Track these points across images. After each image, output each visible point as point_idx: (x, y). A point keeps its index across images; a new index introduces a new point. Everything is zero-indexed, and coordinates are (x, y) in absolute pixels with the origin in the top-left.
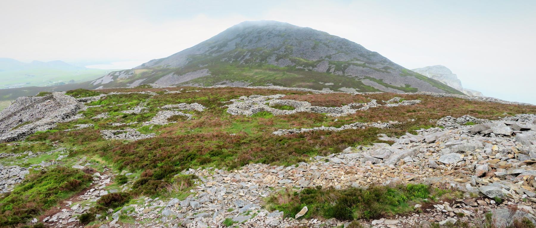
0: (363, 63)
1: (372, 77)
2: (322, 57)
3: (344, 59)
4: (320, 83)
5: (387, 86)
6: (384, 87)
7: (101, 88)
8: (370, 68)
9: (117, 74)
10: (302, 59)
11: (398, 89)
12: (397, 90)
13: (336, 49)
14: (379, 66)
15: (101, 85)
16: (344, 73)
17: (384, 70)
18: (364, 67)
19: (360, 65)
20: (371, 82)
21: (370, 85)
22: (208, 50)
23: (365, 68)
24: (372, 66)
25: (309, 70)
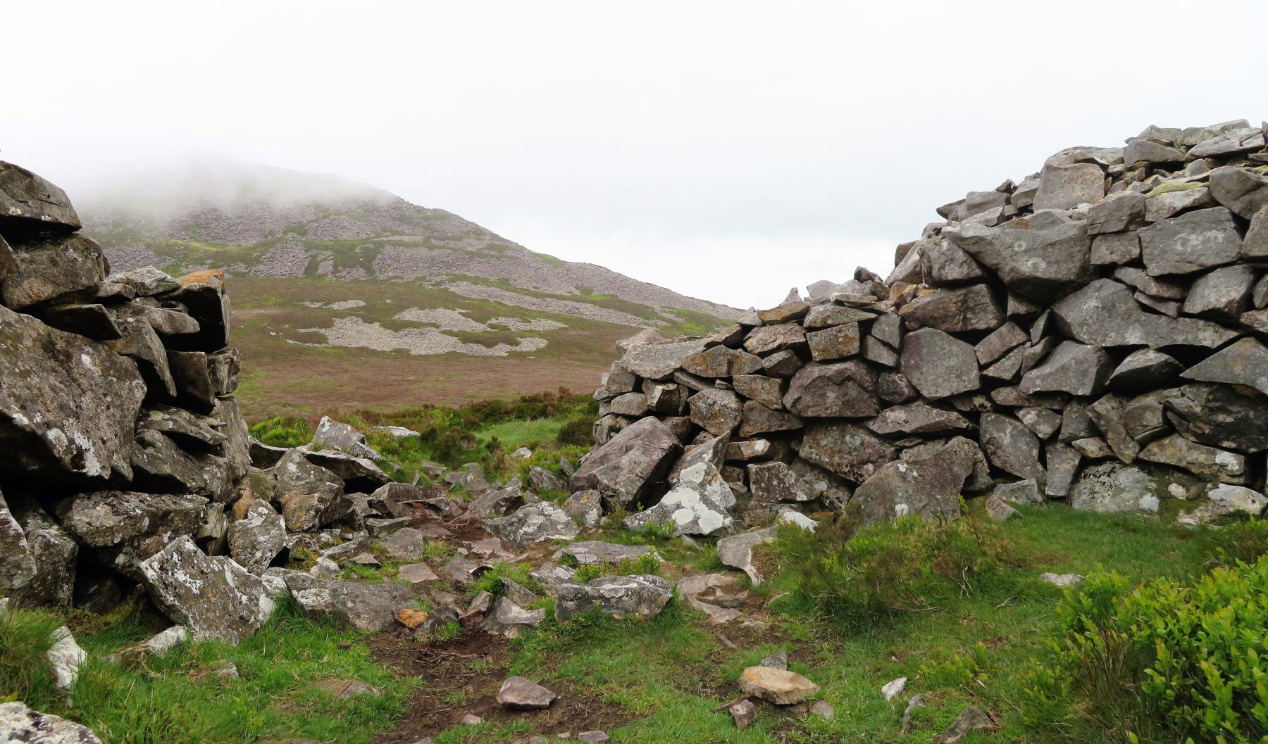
0: (419, 239)
1: (468, 273)
2: (271, 233)
4: (308, 304)
10: (196, 244)
14: (473, 245)
16: (370, 271)
18: (432, 248)
19: (416, 245)
21: (484, 296)
23: (436, 252)
24: (452, 244)
25: (236, 274)
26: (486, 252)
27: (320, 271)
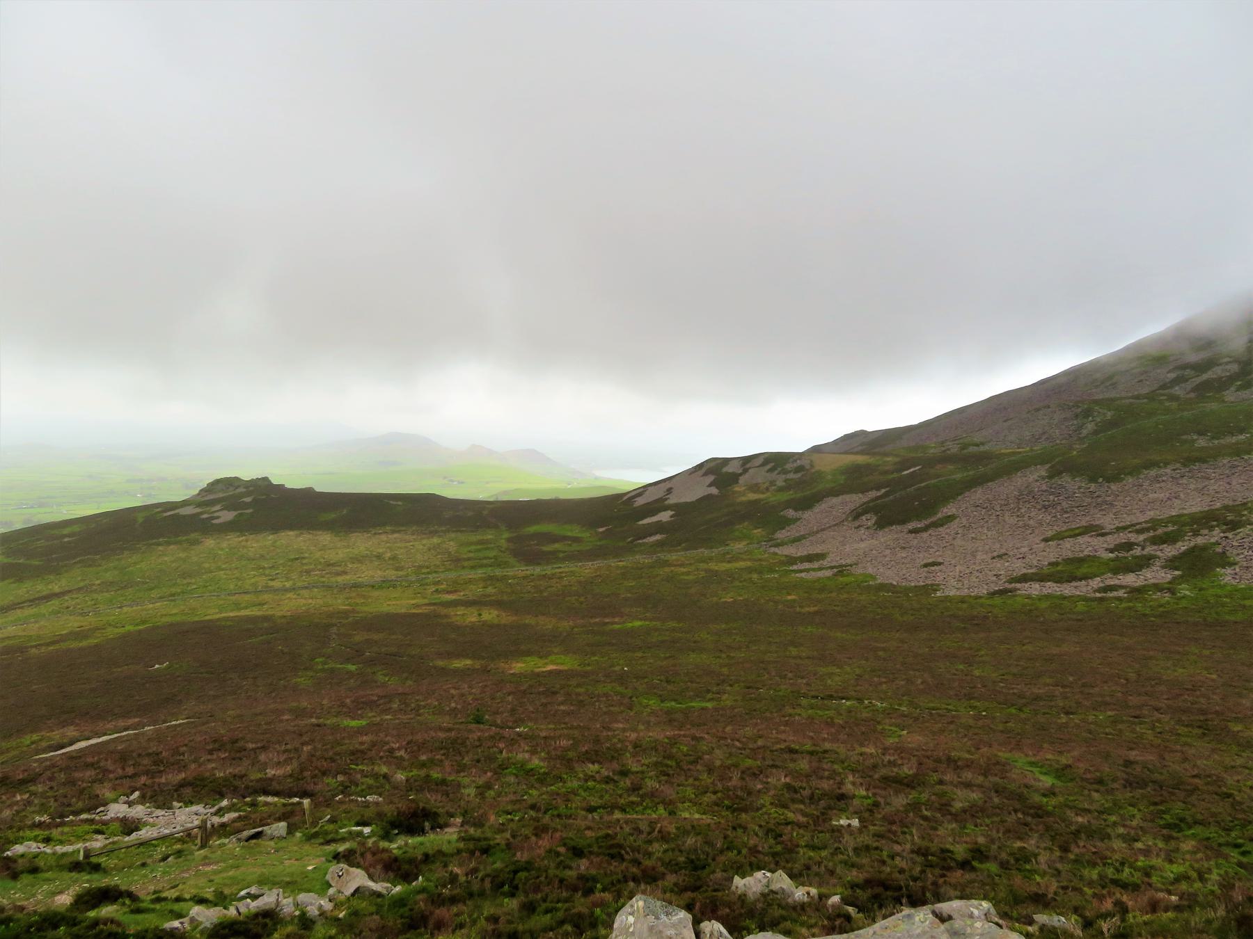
7: (665, 516)
9: (729, 469)
15: (666, 509)
22: (1179, 380)
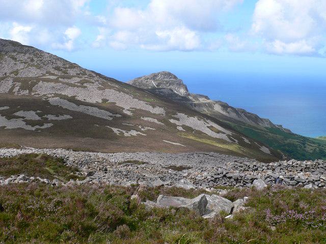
0: (55, 77)
1: (63, 94)
2: (5, 74)
3: (33, 73)
5: (79, 103)
6: (74, 105)
8: (63, 83)
11: (92, 105)
12: (90, 107)
13: (25, 63)
17: (79, 84)
20: (62, 100)
24: (66, 80)
26: (76, 84)
27: (14, 91)
